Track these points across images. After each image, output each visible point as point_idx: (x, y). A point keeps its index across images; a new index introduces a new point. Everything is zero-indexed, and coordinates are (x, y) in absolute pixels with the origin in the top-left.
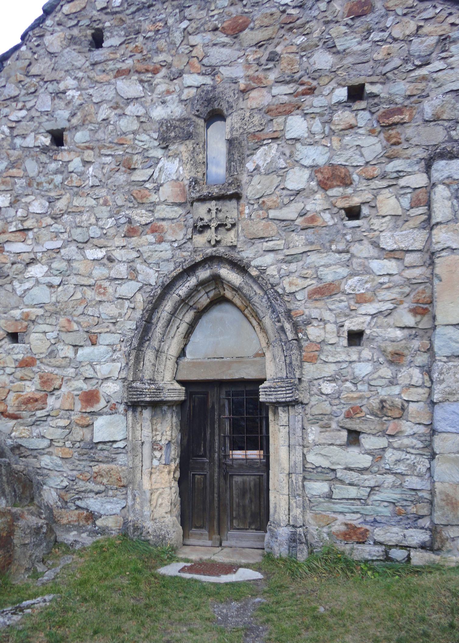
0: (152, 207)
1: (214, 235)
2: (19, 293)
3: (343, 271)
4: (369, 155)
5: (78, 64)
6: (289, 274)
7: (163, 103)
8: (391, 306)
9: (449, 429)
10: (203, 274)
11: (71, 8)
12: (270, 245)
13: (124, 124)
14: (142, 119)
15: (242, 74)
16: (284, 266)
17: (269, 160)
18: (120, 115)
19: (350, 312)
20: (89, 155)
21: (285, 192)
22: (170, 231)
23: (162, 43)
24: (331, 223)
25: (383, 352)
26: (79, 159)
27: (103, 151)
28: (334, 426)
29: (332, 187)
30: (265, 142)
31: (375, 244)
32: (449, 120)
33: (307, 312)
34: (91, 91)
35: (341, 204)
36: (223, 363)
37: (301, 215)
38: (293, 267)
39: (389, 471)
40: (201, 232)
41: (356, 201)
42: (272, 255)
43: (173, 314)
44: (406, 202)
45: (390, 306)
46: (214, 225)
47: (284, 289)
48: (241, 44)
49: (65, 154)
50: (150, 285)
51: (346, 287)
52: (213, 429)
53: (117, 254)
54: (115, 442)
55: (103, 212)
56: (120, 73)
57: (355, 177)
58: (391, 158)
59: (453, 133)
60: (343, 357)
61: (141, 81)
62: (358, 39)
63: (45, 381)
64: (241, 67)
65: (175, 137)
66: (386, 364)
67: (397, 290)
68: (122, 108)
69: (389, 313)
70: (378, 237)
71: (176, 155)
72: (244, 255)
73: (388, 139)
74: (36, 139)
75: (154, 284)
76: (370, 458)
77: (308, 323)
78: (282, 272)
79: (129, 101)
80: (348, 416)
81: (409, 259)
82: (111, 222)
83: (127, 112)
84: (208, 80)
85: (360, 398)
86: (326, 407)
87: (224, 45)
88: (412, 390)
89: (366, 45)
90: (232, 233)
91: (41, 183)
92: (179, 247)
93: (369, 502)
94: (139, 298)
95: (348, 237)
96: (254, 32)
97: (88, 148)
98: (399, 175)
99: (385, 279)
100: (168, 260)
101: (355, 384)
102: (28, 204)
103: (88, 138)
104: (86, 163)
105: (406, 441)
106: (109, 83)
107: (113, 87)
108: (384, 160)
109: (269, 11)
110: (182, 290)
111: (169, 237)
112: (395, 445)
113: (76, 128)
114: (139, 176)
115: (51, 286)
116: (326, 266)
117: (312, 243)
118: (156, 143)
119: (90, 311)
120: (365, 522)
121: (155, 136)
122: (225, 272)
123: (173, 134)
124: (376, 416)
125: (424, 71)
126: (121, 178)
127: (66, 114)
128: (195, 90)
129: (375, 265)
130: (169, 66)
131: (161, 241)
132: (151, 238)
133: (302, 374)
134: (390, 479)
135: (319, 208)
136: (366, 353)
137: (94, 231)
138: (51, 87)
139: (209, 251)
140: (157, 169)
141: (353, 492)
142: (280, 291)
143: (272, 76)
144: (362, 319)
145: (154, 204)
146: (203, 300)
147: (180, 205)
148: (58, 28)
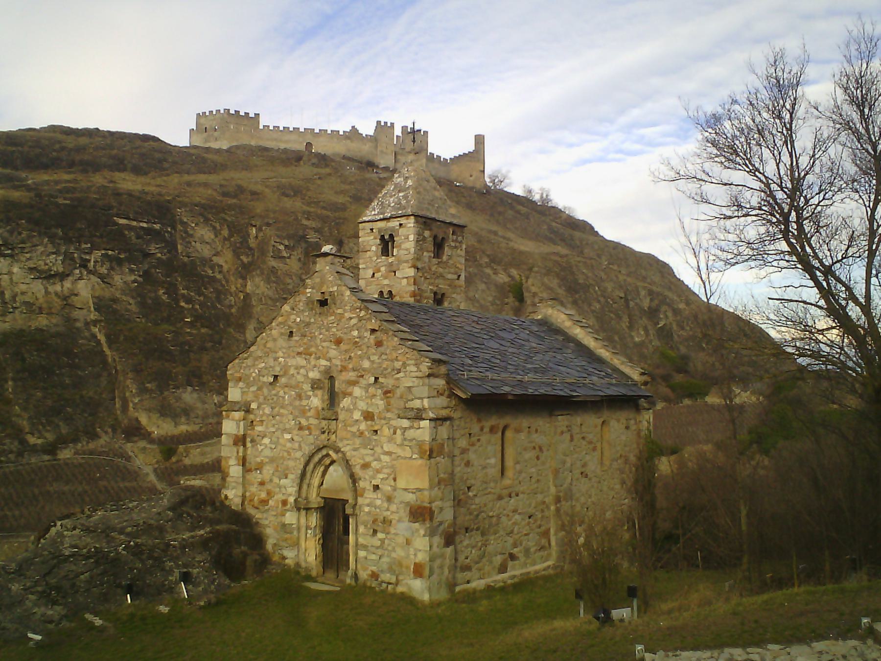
0: (307, 419)
2: (260, 450)
5: (284, 346)
7: (313, 370)
8: (387, 476)
10: (324, 452)
13: (300, 378)
19: (374, 477)
20: (286, 389)
31: (382, 447)
41: (376, 428)
43: (315, 467)
46: (327, 432)
53: (296, 438)
54: (293, 524)
55: (291, 417)
56: (299, 353)
57: (376, 418)
58: (388, 411)
61: (306, 359)
63: (269, 493)
69: (387, 478)
72: (339, 445)
74: (268, 378)
84: (328, 363)
85: (376, 515)
87: (334, 349)
89: (380, 361)
94: (302, 459)
98: (390, 419)
99: (385, 464)
101: (375, 509)
102: (264, 408)
104: (285, 393)
110: (316, 459)
111: (313, 433)
113: (282, 376)
114: (304, 403)
115: (271, 448)
116: (367, 455)
118: (310, 389)
119: (285, 463)
121: (310, 385)
126: (297, 403)
129: (382, 457)
131: (310, 434)
132: (307, 432)
137: (287, 426)
138: (274, 355)
143: (351, 366)
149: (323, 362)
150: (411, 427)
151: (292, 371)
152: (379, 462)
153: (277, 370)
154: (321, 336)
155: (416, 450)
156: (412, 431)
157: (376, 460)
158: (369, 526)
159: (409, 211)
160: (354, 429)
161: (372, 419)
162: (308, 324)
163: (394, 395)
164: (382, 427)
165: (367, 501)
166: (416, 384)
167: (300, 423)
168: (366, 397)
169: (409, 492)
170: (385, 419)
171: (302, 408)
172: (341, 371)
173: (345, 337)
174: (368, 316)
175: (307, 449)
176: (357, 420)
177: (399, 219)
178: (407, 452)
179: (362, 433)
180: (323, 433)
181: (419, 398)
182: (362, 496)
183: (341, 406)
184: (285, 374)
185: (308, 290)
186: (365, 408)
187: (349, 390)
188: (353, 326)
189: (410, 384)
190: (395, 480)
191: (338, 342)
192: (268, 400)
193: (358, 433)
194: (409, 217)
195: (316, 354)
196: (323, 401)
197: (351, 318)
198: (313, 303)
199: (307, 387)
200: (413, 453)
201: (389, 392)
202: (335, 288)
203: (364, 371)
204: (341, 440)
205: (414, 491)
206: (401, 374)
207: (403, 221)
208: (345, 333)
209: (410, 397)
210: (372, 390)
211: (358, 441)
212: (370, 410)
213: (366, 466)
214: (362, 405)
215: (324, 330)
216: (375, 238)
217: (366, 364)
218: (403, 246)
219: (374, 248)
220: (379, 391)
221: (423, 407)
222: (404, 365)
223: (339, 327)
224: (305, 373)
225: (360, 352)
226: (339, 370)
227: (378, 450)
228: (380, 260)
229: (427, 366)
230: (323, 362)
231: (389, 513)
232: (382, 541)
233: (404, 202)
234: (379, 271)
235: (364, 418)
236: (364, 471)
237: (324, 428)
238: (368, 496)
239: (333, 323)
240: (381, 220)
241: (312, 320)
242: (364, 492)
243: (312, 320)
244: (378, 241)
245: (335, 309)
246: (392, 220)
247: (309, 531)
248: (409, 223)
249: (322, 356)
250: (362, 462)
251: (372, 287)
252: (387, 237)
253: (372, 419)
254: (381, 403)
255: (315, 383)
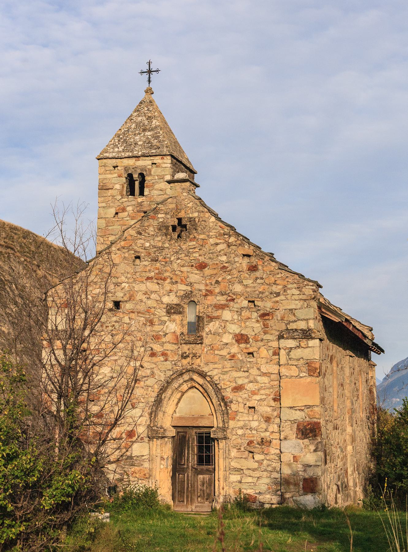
0: (162, 344)
1: (191, 361)
3: (246, 381)
4: (256, 331)
6: (223, 380)
7: (169, 295)
8: (265, 397)
9: (286, 451)
11: (125, 244)
12: (216, 366)
13: (150, 303)
14: (159, 302)
15: (204, 288)
16: (221, 376)
17: (215, 328)
18: (148, 298)
20: (133, 316)
21: (222, 343)
22: (171, 356)
23: (168, 268)
24: (241, 359)
25: (263, 417)
26: (128, 317)
27: (139, 314)
28: (242, 449)
29: (242, 343)
30: (214, 320)
31: (259, 369)
32: (287, 321)
33: (231, 398)
34: (134, 285)
35: (245, 351)
36: (194, 417)
37: (229, 354)
38: (225, 377)
39: (265, 470)
40: (185, 359)
41: (251, 350)
42: (216, 370)
44: (271, 352)
45: (264, 397)
46: (191, 356)
47: (221, 386)
48: (204, 274)
49: (121, 313)
50: (161, 381)
51: (247, 388)
52: (188, 450)
53: (145, 365)
54: (143, 456)
56: (148, 278)
57: (251, 340)
58: (265, 333)
59: (288, 326)
60: (246, 418)
61: (158, 284)
62: (252, 281)
64: (203, 285)
65: (174, 313)
66: (264, 422)
67: (267, 390)
68: (149, 295)
69: (265, 400)
70: (260, 367)
71: (174, 321)
72: (204, 369)
73: (264, 325)
75: (163, 380)
76: (257, 464)
77: (231, 402)
78: (221, 378)
79: (152, 292)
80: (248, 444)
81: (273, 377)
82: (142, 349)
83: (151, 297)
84: (189, 288)
86: (239, 441)
88: (274, 434)
90: (199, 360)
91: (108, 326)
92: (175, 364)
93: (257, 484)
94: (156, 386)
95: (248, 366)
96: (209, 270)
97: (132, 312)
99: (263, 385)
100: (169, 370)
103: (132, 307)
105: (272, 457)
106: (142, 282)
107: (145, 285)
108: (262, 333)
109: (216, 262)
111: (170, 359)
112: (268, 458)
114: (157, 328)
116: (239, 378)
117: (233, 367)
118: (165, 314)
120: (256, 493)
121: (165, 310)
122: (196, 377)
123: (173, 311)
124: (260, 445)
125: (278, 299)
126: (148, 329)
127: (122, 295)
128: (183, 292)
129: (259, 378)
130: (171, 279)
131: (166, 360)
132: (162, 358)
133: (228, 425)
134: (265, 473)
135: (236, 352)
136: (256, 417)
139: (189, 367)
140: (165, 326)
141: (250, 480)
142: (220, 387)
143: (217, 290)
144: (253, 401)
145: (163, 343)
146: (185, 387)
147: (175, 344)
148: (118, 252)
149: (182, 287)
150: (299, 347)
151: (140, 296)
152: (256, 384)
153: (119, 296)
154: (179, 261)
155: (304, 369)
156: (299, 350)
157: (251, 382)
158: (242, 449)
159: (165, 151)
160: (224, 352)
161: (247, 341)
162: (162, 249)
163: (273, 317)
164: (259, 349)
165: (241, 424)
166: (298, 307)
167: (152, 349)
168: (238, 320)
169: (296, 410)
170: (262, 340)
171: (154, 334)
172: (206, 295)
173: (210, 262)
174: (239, 242)
175: (161, 376)
176: (227, 344)
177: (152, 158)
178: (294, 371)
179: (233, 356)
180: (185, 358)
181: (304, 320)
182: (234, 419)
183: (207, 330)
184: (131, 298)
185: (160, 216)
186: (237, 331)
187: (216, 314)
188: (220, 252)
189: (293, 307)
190: (277, 399)
191: (202, 266)
192: (107, 327)
193: (228, 356)
194: (165, 158)
195: (171, 279)
196: (183, 326)
197: (217, 244)
198: (167, 228)
199: (161, 312)
200: (301, 371)
201: (268, 314)
202: (196, 215)
203: (234, 294)
204: (207, 364)
205: (303, 408)
206: (282, 297)
207: (157, 160)
208: (210, 258)
209: (292, 318)
210: (245, 314)
211: (228, 364)
212: (243, 332)
213: (238, 389)
214: (234, 329)
215: (183, 255)
216: (120, 176)
217: (238, 288)
218: (157, 186)
219: (118, 187)
220: (255, 315)
221: (308, 328)
222: (285, 289)
223: (201, 252)
224: (158, 298)
225: (229, 277)
226: (204, 294)
227: (254, 371)
228: (126, 199)
229: (312, 289)
230: (182, 287)
231: (268, 434)
232: (260, 463)
233: (155, 142)
234: (124, 210)
235: (236, 341)
236: (236, 394)
237: (186, 353)
238: (241, 419)
239: (194, 248)
240: (129, 157)
241: (167, 245)
242: (237, 415)
243: (167, 245)
244: (124, 180)
245: (196, 234)
246: (142, 158)
247: (162, 462)
248: (165, 163)
249: (179, 281)
250: (234, 385)
251: (114, 227)
252: (135, 176)
253: (247, 341)
254: (258, 327)
255: (172, 308)
